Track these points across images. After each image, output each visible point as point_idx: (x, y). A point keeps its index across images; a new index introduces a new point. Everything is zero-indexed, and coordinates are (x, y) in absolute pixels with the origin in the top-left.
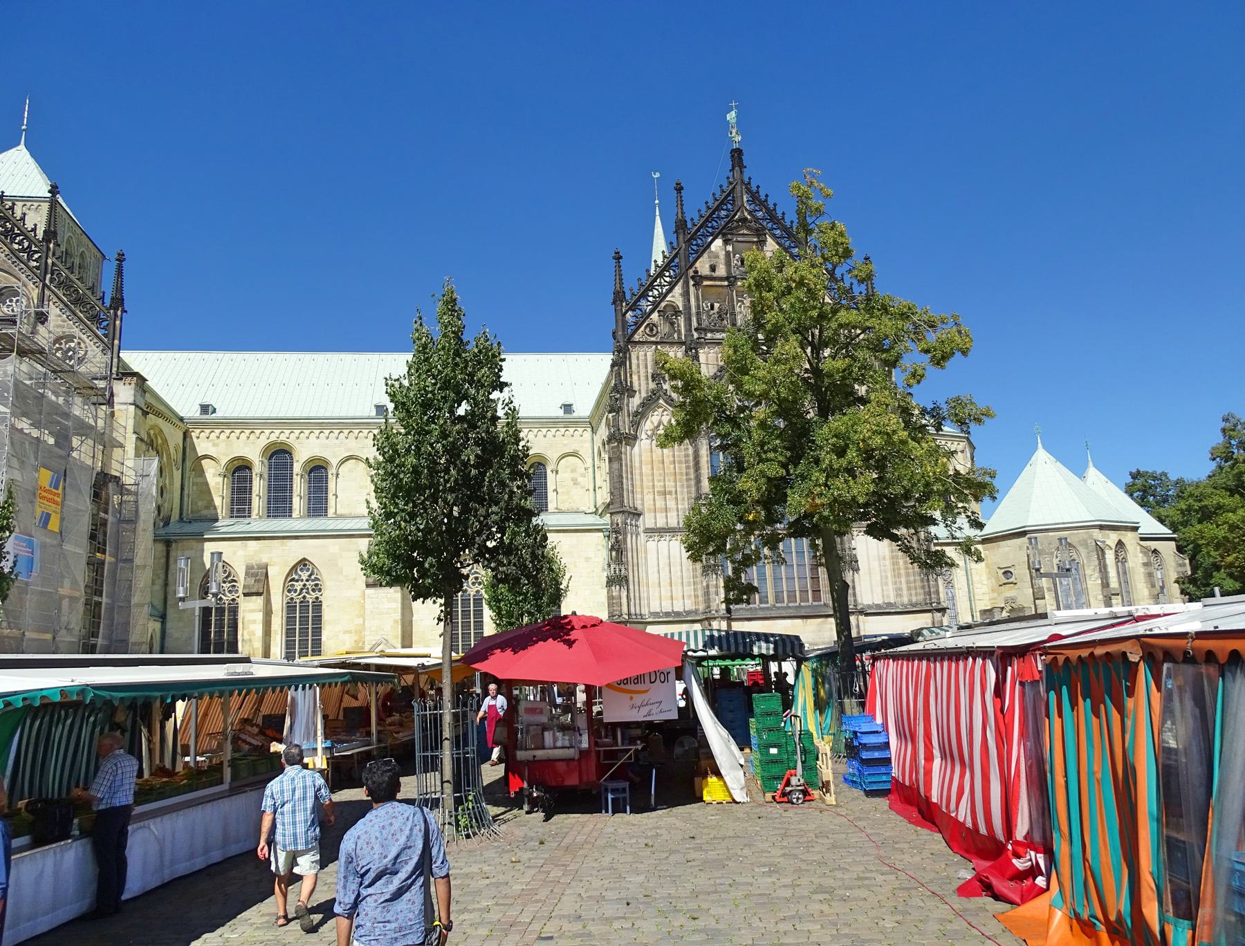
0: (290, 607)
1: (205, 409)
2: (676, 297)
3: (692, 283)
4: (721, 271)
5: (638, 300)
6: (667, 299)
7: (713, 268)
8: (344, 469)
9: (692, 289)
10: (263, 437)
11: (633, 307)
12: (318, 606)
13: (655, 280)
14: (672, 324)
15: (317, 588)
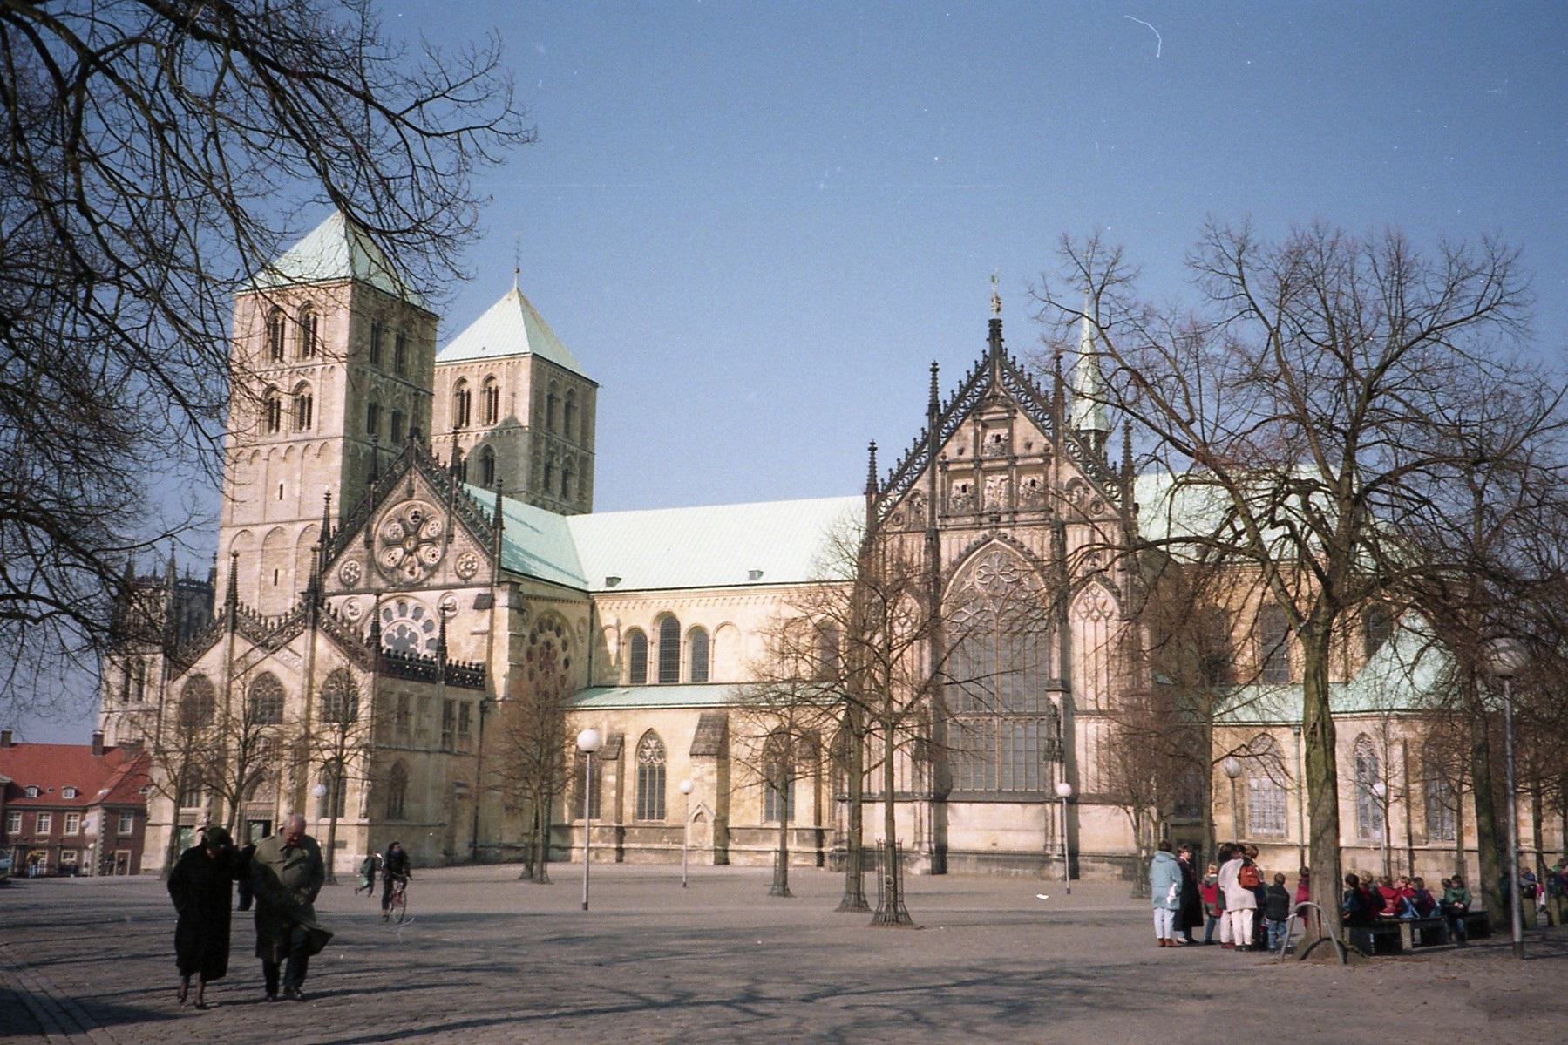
0: (642, 773)
1: (611, 581)
2: (922, 485)
3: (938, 468)
4: (969, 454)
5: (889, 490)
6: (915, 487)
7: (961, 452)
8: (719, 637)
9: (939, 476)
10: (653, 607)
11: (883, 496)
12: (663, 773)
13: (905, 468)
14: (918, 512)
15: (662, 755)
